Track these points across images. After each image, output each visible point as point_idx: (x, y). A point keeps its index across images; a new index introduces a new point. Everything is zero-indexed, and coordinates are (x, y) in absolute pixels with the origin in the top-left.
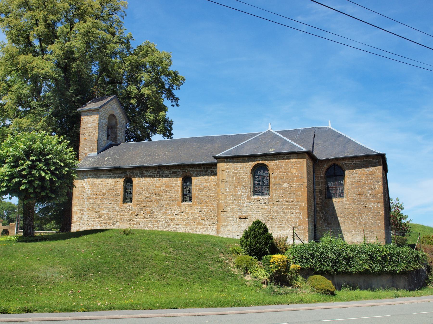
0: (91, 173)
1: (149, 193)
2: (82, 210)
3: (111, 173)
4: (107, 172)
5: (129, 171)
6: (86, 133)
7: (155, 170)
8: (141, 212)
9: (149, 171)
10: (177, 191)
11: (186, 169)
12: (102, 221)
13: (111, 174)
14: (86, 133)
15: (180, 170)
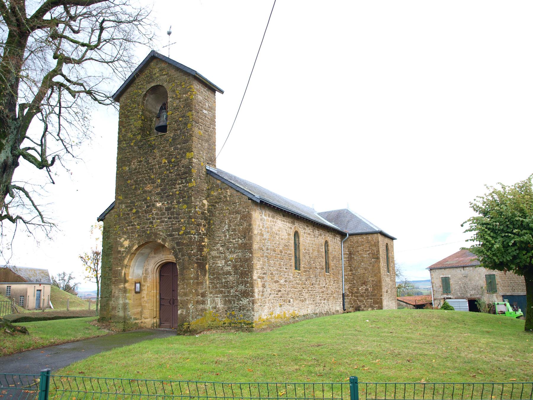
0: (270, 213)
1: (310, 257)
2: (263, 278)
3: (285, 219)
4: (282, 216)
5: (297, 223)
6: (201, 124)
7: (312, 228)
8: (306, 282)
9: (309, 227)
10: (323, 258)
11: (326, 233)
12: (282, 299)
13: (284, 221)
14: (201, 124)
15: (324, 233)
